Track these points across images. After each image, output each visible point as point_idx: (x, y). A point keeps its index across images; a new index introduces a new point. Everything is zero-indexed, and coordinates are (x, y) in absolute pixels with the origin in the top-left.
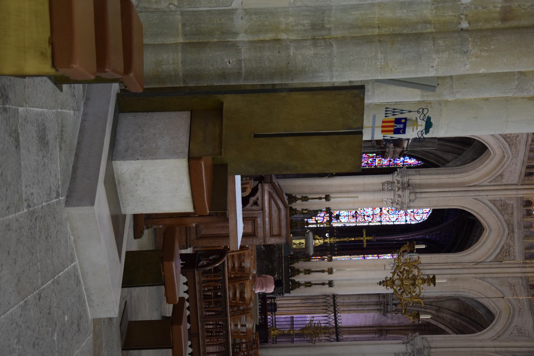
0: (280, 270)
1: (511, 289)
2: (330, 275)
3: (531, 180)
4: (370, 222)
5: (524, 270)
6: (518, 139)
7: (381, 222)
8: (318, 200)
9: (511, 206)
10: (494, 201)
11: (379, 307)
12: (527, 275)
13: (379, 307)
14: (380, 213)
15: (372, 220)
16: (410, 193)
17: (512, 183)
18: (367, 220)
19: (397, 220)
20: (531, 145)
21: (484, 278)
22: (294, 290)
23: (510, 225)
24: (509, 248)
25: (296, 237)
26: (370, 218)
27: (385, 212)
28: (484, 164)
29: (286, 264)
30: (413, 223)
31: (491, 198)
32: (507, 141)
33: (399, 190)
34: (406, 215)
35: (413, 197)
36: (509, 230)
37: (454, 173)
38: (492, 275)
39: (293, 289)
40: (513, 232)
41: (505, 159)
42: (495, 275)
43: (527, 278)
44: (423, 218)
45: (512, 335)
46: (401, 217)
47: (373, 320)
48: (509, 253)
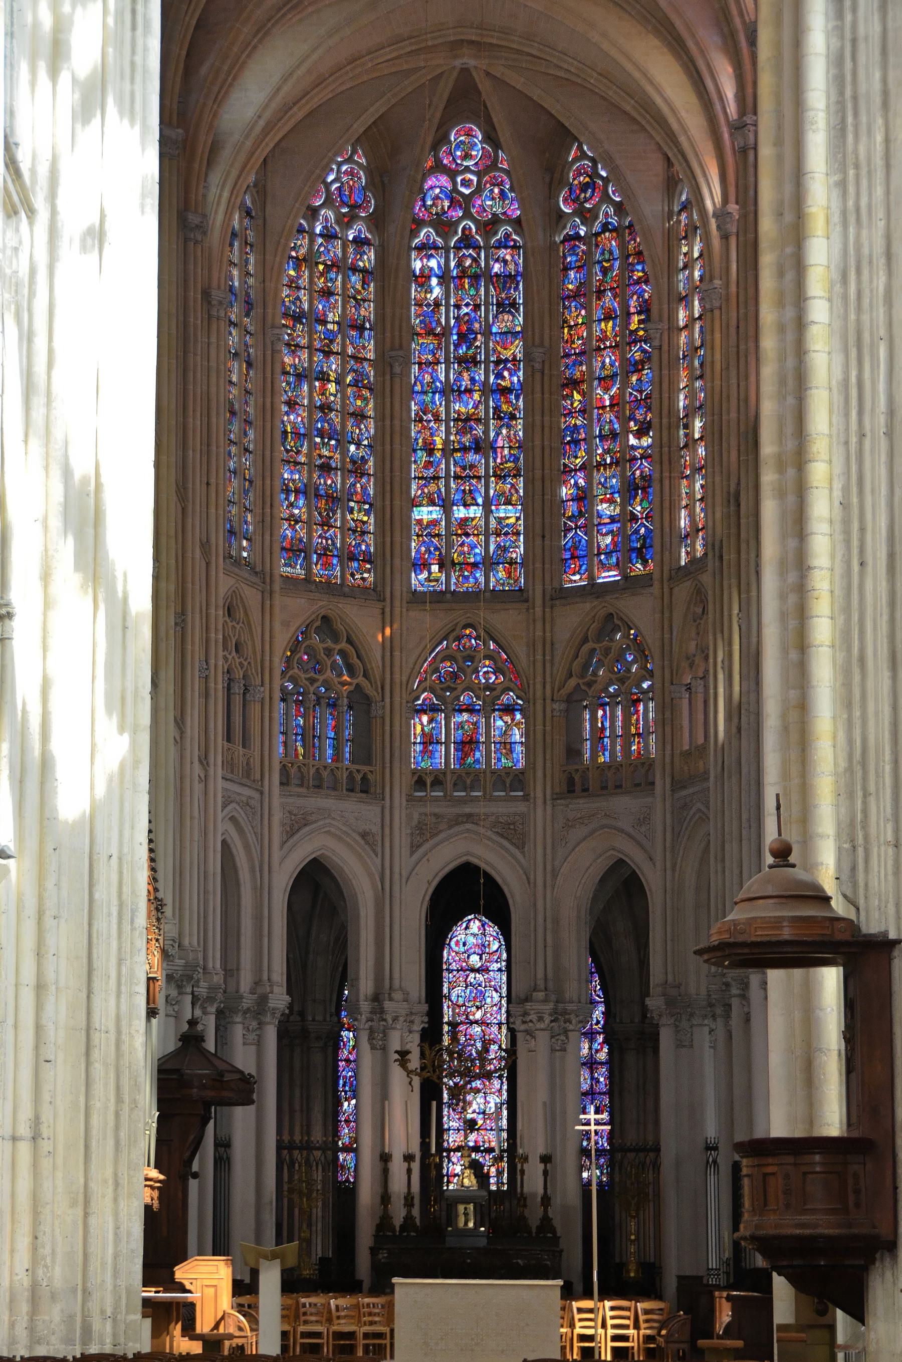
5: (540, 802)
7: (500, 1024)
10: (412, 847)
12: (548, 797)
16: (391, 999)
17: (380, 816)
20: (308, 788)
21: (553, 870)
23: (457, 821)
27: (478, 1015)
30: (505, 956)
31: (406, 851)
32: (298, 830)
33: (385, 1020)
34: (487, 970)
35: (398, 996)
38: (549, 857)
40: (470, 815)
41: (332, 830)
42: (549, 851)
44: (495, 934)
46: (490, 981)
48: (509, 824)
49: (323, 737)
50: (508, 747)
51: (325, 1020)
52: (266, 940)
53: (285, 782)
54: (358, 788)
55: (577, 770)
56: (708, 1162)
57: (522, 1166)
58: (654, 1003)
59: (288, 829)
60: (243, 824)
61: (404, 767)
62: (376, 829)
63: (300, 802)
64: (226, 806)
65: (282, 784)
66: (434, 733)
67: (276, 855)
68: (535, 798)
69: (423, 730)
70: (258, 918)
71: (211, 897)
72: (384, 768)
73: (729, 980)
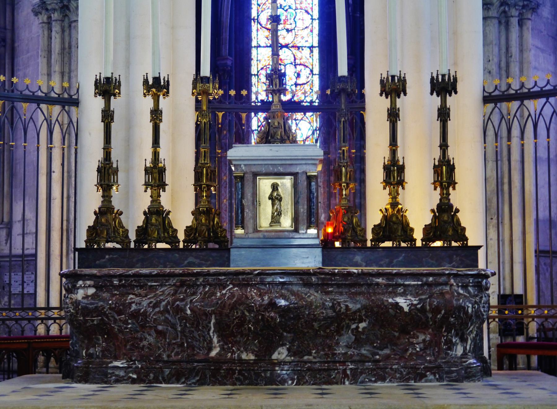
0: (378, 284)
2: (408, 90)
4: (312, 71)
7: (311, 48)
8: (114, 126)
11: (514, 21)
13: (514, 21)
14: (292, 49)
15: (307, 67)
18: (308, 77)
19: (310, 11)
22: (464, 229)
25: (248, 213)
26: (303, 71)
29: (358, 258)
47: (543, 51)
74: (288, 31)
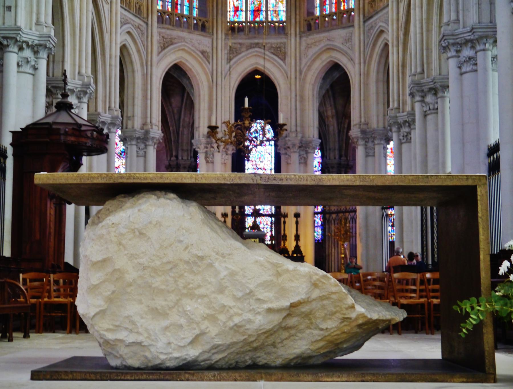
1: (311, 47)
3: (209, 26)
6: (166, 37)
9: (234, 45)
12: (298, 33)
17: (211, 43)
19: (270, 153)
20: (173, 26)
23: (251, 46)
24: (273, 47)
28: (191, 67)
31: (224, 62)
32: (167, 47)
36: (256, 47)
37: (199, 95)
39: (300, 252)
41: (186, 48)
43: (301, 33)
45: (350, 48)
48: (277, 48)
49: (182, 5)
50: (277, 13)
51: (188, 159)
52: (149, 102)
53: (161, 20)
54: (200, 29)
55: (312, 19)
56: (383, 215)
57: (284, 219)
58: (354, 132)
59: (162, 45)
60: (136, 38)
61: (223, 19)
62: (209, 50)
63: (169, 32)
64: (125, 24)
65: (158, 22)
66: (239, 6)
67: (155, 58)
68: (291, 34)
69: (234, 5)
70: (145, 90)
71: (113, 68)
72: (213, 19)
73: (415, 91)
74: (261, 162)
